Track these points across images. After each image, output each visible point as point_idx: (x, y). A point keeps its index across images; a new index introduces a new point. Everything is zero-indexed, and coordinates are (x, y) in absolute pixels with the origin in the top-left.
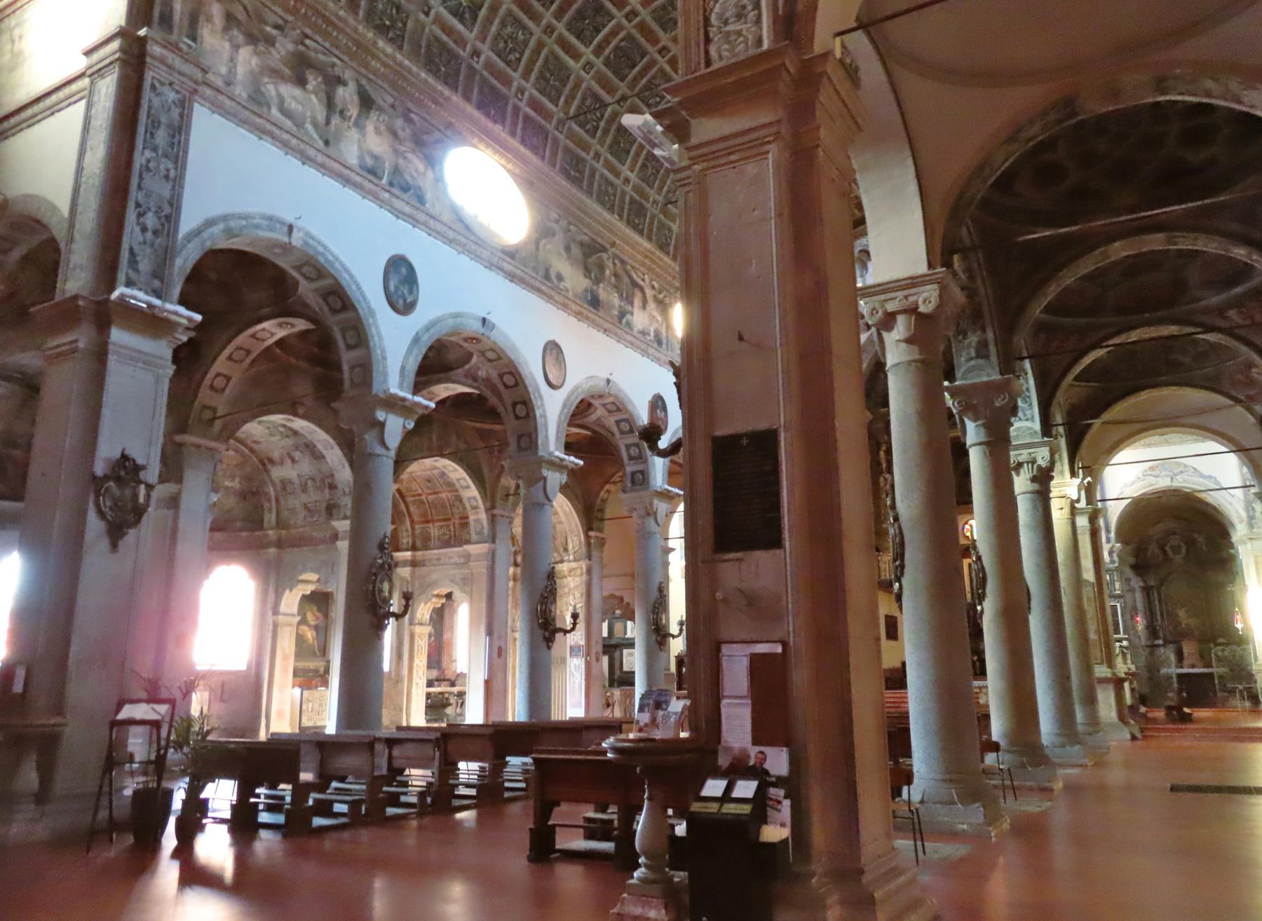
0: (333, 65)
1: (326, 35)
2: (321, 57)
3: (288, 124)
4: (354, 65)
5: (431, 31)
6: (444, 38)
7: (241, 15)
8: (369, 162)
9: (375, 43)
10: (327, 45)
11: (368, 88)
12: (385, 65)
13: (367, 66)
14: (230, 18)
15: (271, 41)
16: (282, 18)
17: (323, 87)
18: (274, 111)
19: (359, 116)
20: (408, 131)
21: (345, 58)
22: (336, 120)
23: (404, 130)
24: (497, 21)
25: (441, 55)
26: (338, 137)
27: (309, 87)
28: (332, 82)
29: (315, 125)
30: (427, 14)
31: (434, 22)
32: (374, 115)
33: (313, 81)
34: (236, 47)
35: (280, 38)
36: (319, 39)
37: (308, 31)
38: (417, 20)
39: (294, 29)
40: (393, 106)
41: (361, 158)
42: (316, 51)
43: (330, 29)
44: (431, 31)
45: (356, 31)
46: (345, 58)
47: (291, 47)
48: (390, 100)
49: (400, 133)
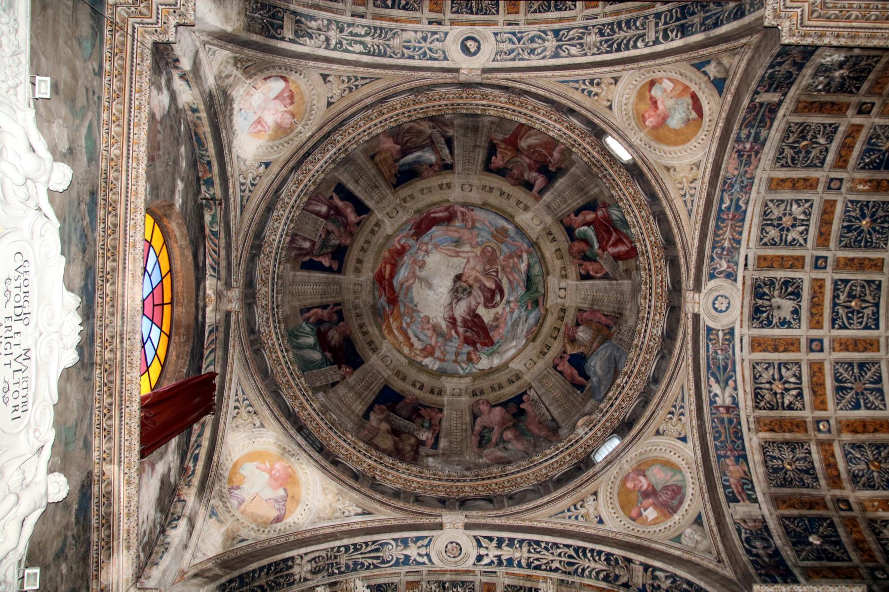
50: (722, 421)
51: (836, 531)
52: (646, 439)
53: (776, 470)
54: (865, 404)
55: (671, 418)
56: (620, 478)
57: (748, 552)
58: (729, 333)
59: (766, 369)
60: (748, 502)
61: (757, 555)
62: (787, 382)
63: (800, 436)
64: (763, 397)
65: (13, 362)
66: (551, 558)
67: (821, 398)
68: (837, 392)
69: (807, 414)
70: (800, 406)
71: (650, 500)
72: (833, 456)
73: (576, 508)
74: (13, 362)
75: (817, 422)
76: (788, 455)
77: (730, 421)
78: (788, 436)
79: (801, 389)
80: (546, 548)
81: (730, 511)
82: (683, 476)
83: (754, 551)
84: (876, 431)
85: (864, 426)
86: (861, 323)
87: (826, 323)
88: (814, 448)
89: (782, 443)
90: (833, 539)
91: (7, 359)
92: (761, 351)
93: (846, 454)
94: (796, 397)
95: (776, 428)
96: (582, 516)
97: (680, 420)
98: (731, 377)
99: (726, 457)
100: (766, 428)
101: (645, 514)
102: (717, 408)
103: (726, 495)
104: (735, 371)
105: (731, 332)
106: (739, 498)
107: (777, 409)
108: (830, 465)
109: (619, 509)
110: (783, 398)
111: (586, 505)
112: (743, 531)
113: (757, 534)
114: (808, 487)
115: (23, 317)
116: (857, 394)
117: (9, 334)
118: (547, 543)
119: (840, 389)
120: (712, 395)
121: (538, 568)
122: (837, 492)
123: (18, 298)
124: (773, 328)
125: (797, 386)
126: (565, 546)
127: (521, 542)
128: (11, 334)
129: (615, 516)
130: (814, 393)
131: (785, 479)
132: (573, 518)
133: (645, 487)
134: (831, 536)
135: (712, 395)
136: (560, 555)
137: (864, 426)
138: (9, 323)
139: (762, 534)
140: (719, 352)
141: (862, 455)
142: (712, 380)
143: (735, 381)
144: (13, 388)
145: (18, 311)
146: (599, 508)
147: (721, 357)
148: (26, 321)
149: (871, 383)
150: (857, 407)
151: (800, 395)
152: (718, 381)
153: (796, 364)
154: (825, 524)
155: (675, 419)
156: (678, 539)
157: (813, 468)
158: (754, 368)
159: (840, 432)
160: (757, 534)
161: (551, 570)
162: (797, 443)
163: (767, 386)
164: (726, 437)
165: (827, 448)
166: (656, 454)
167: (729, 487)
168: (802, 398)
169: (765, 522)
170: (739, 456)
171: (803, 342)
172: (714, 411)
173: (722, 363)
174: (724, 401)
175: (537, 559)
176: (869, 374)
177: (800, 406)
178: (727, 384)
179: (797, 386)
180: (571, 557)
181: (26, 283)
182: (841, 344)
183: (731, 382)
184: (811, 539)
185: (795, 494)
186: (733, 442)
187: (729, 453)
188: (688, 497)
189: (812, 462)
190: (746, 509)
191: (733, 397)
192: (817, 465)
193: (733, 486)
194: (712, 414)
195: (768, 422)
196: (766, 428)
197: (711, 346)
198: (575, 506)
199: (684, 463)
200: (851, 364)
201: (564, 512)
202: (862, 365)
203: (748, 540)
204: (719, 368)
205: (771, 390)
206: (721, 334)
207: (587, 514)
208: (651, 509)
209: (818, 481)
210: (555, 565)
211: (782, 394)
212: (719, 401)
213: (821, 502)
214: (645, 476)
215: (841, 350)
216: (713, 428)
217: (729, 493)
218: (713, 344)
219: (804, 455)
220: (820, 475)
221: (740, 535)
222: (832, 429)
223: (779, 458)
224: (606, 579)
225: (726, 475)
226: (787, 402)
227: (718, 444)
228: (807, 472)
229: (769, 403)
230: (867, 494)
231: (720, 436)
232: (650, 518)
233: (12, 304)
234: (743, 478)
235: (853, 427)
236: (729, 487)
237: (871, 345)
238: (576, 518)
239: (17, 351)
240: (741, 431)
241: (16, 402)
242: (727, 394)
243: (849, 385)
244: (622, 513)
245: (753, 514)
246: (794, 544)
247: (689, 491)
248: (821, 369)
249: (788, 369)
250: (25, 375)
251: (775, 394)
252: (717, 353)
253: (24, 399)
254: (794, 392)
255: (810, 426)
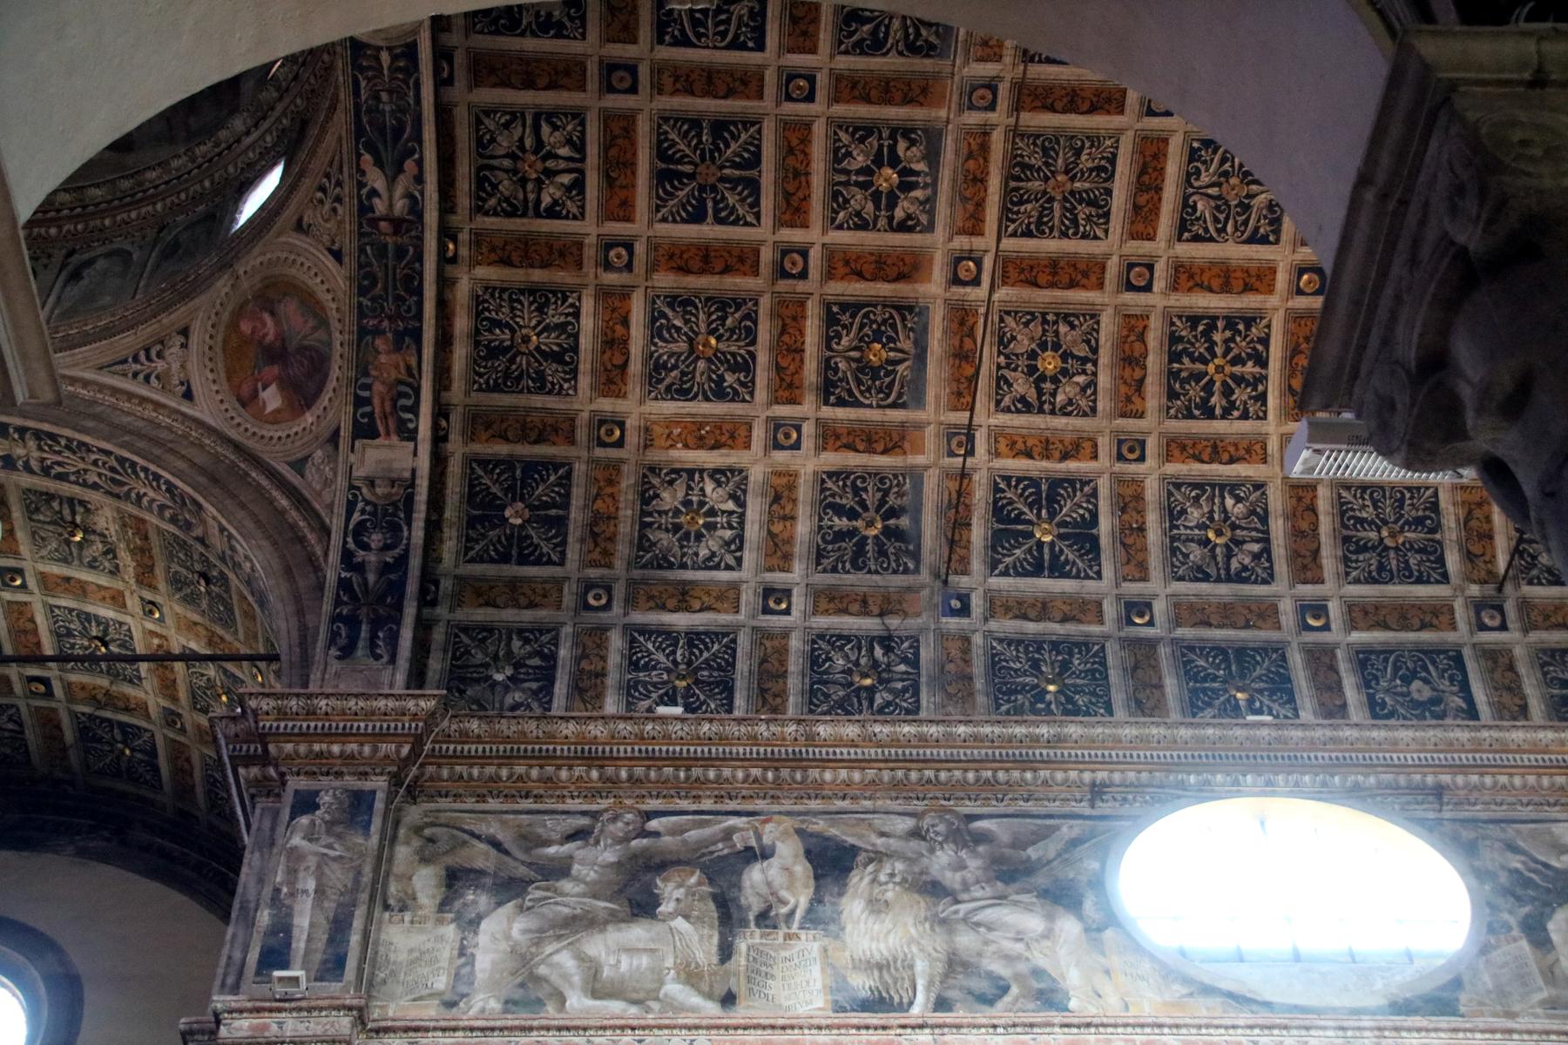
0: (728, 834)
1: (693, 788)
2: (693, 835)
3: (616, 1006)
4: (787, 805)
5: (988, 635)
6: (1031, 627)
7: (480, 856)
8: (862, 984)
9: (811, 738)
10: (707, 804)
11: (833, 831)
12: (853, 764)
13: (818, 790)
14: (455, 879)
15: (560, 869)
16: (584, 813)
17: (707, 889)
18: (577, 1002)
19: (817, 900)
20: (974, 864)
21: (760, 805)
22: (748, 940)
23: (961, 866)
24: (1152, 519)
25: (1036, 665)
26: (759, 971)
27: (666, 908)
28: (722, 873)
29: (691, 976)
30: (965, 611)
31: (991, 613)
32: (859, 881)
33: (671, 892)
34: (474, 924)
35: (579, 854)
36: (684, 804)
37: (654, 804)
38: (942, 636)
39: (615, 819)
40: (916, 834)
41: (837, 985)
42: (677, 831)
43: (696, 772)
44: (988, 635)
45: (754, 739)
46: (760, 805)
47: (610, 856)
48: (909, 823)
49: (952, 879)
50: (382, 251)
51: (568, 495)
52: (279, 235)
53: (494, 352)
54: (717, 211)
55: (321, 202)
56: (230, 308)
57: (347, 556)
58: (403, 55)
59: (507, 126)
60: (395, 439)
61: (360, 568)
62: (552, 155)
63: (562, 277)
64: (495, 186)
66: (82, 466)
67: (623, 194)
68: (660, 183)
69: (589, 229)
70: (574, 210)
71: (276, 369)
72: (625, 322)
73: (149, 358)
75: (608, 245)
76: (527, 318)
77: (401, 252)
78: (538, 275)
79: (582, 172)
80: (68, 447)
81: (352, 458)
82: (330, 335)
83: (361, 554)
84: (727, 270)
85: (706, 259)
86: (724, 34)
87: (645, 32)
88: (587, 305)
89: (522, 292)
90: (553, 512)
92: (494, 86)
93: (654, 317)
94: (569, 189)
95: (515, 258)
96: (158, 377)
97: (334, 210)
98: (412, 152)
99: (377, 332)
100: (493, 257)
101: (264, 395)
102: (374, 222)
103: (355, 420)
104: (418, 138)
105: (411, 51)
106: (381, 429)
107: (524, 215)
108: (614, 342)
109: (223, 375)
110: (540, 189)
111: (167, 353)
112: (360, 505)
113: (385, 514)
114: (550, 393)
116: (702, 188)
118: (69, 440)
119: (665, 178)
120: (364, 191)
121: (62, 477)
122: (606, 405)
124: (522, 35)
125: (572, 165)
126: (101, 450)
127: (22, 431)
129: (215, 388)
130: (609, 181)
131: (507, 374)
132: (141, 376)
133: (270, 338)
134: (554, 505)
135: (364, 191)
136: (95, 463)
137: (706, 259)
139: (394, 515)
140: (384, 96)
141: (687, 322)
142: (367, 157)
143: (420, 163)
146: (189, 365)
147: (387, 108)
149: (735, 166)
150: (697, 217)
151: (579, 185)
152: (379, 163)
153: (575, 116)
154: (552, 478)
155: (327, 207)
156: (299, 465)
157: (575, 349)
158: (479, 122)
159: (652, 268)
160: (385, 514)
161: (85, 484)
162: (554, 293)
163: (507, 163)
164: (385, 289)
165: (617, 304)
166: (293, 271)
167: (368, 402)
168: (582, 192)
169: (412, 485)
170: (406, 332)
171: (592, 69)
172: (366, 229)
173: (390, 121)
174: (391, 206)
175: (59, 464)
176: (734, 146)
177: (574, 210)
178: (400, 169)
179: (572, 165)
180: (112, 469)
182: (677, 79)
183: (409, 165)
184: (507, 513)
185: (515, 408)
186: (398, 298)
187: (386, 324)
188: (332, 384)
189: (576, 336)
190: (383, 454)
191: (410, 196)
192: (585, 343)
193: (376, 401)
194: (361, 235)
195: (499, 243)
196: (493, 257)
197: (363, 84)
198: (147, 351)
199: (334, 306)
200: (696, 124)
201: (125, 361)
202: (721, 127)
203: (360, 529)
204: (382, 130)
205: (515, 171)
206: (385, 57)
207: (168, 372)
208: (273, 388)
209: (575, 378)
210: (92, 478)
211: (539, 182)
212: (380, 206)
213: (565, 426)
214: (272, 314)
215: (675, 92)
216: (360, 267)
217: (363, 416)
218: (369, 80)
219: (562, 319)
220: (585, 366)
221: (349, 513)
222: (636, 262)
223: (508, 325)
224: (173, 520)
225: (366, 374)
226: (546, 200)
227: (366, 302)
228: (557, 357)
229: (507, 200)
230: (670, 407)
231: (374, 284)
232: (270, 408)
234: (401, 382)
235: (679, 259)
236: (368, 402)
237: (745, 83)
238: (147, 379)
240: (421, 274)
242: (399, 191)
243: (688, 168)
244: (226, 386)
245: (396, 465)
246: (471, 523)
247: (335, 372)
248: (629, 131)
249: (555, 128)
251: (523, 181)
252: (377, 98)
254: (566, 179)
255: (590, 253)
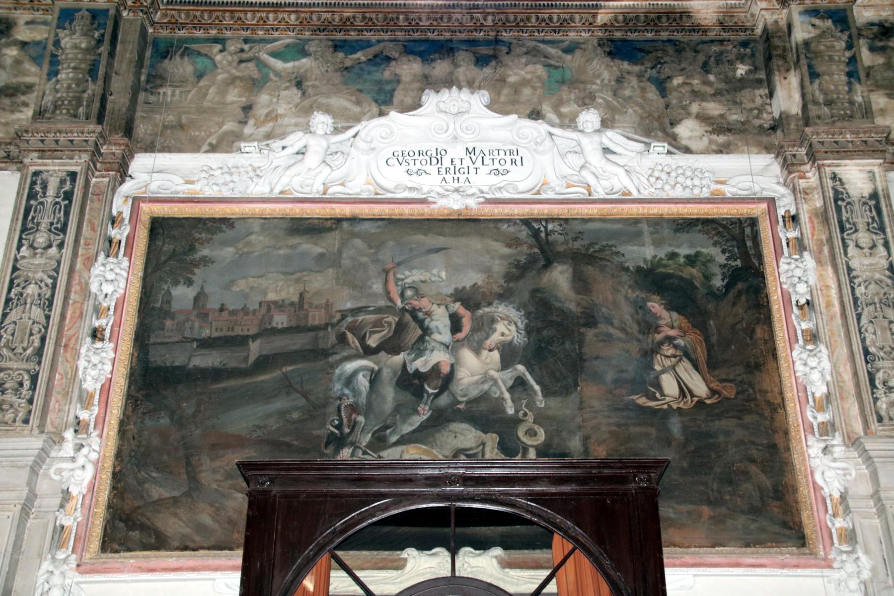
65: (476, 165)
74: (476, 165)
91: (472, 171)
115: (439, 157)
117: (452, 171)
123: (424, 162)
128: (452, 168)
138: (443, 171)
144: (497, 165)
145: (434, 161)
148: (443, 153)
181: (411, 154)
233: (428, 168)
239: (467, 162)
241: (509, 162)
250: (487, 153)
253: (508, 153)
